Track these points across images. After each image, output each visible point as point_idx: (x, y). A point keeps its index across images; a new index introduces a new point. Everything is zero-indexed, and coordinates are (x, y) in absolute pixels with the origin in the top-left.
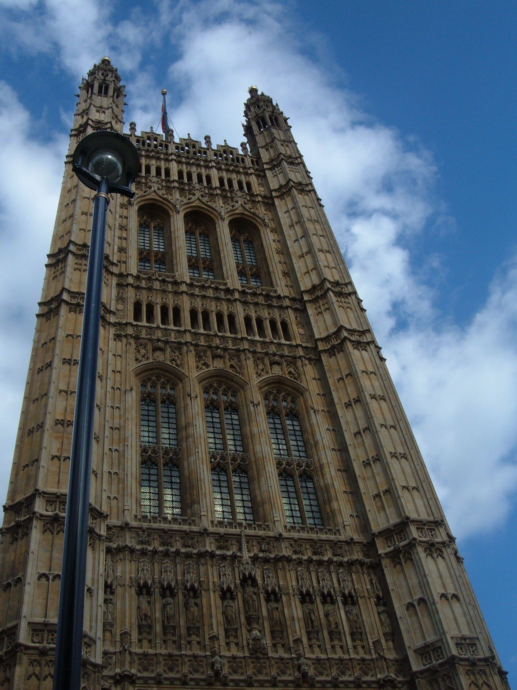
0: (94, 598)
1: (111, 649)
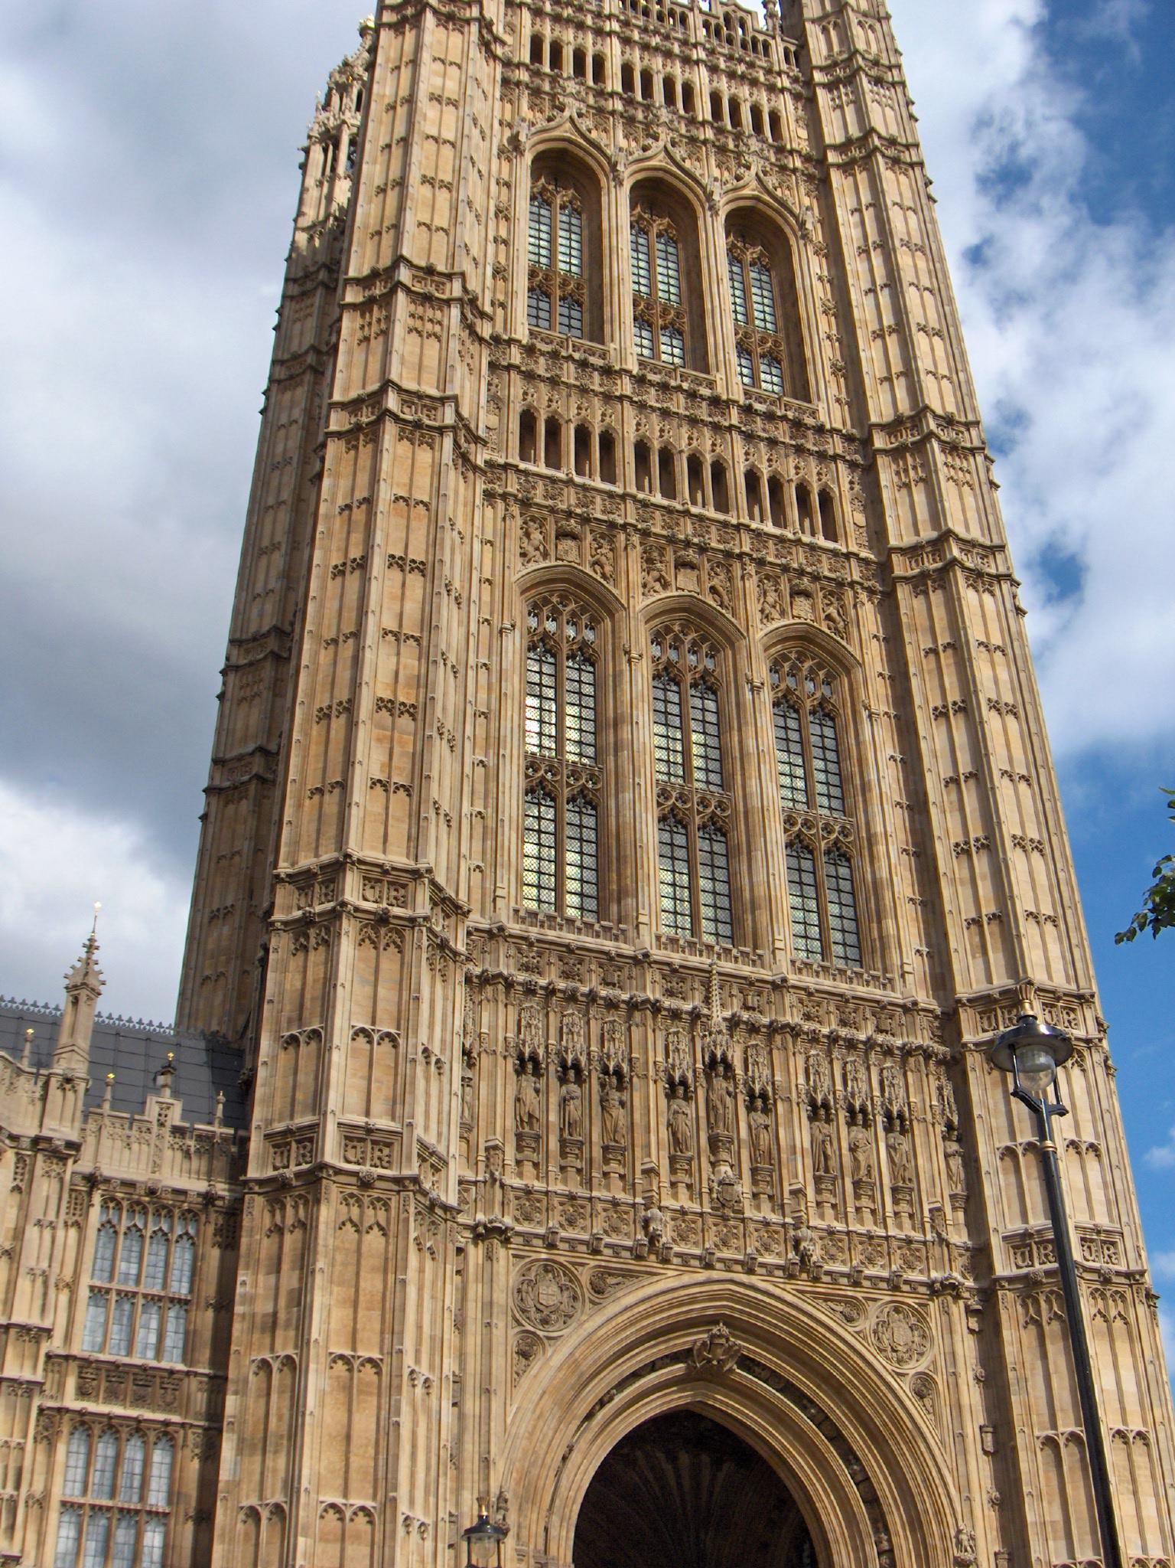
0: (445, 1079)
1: (470, 1176)
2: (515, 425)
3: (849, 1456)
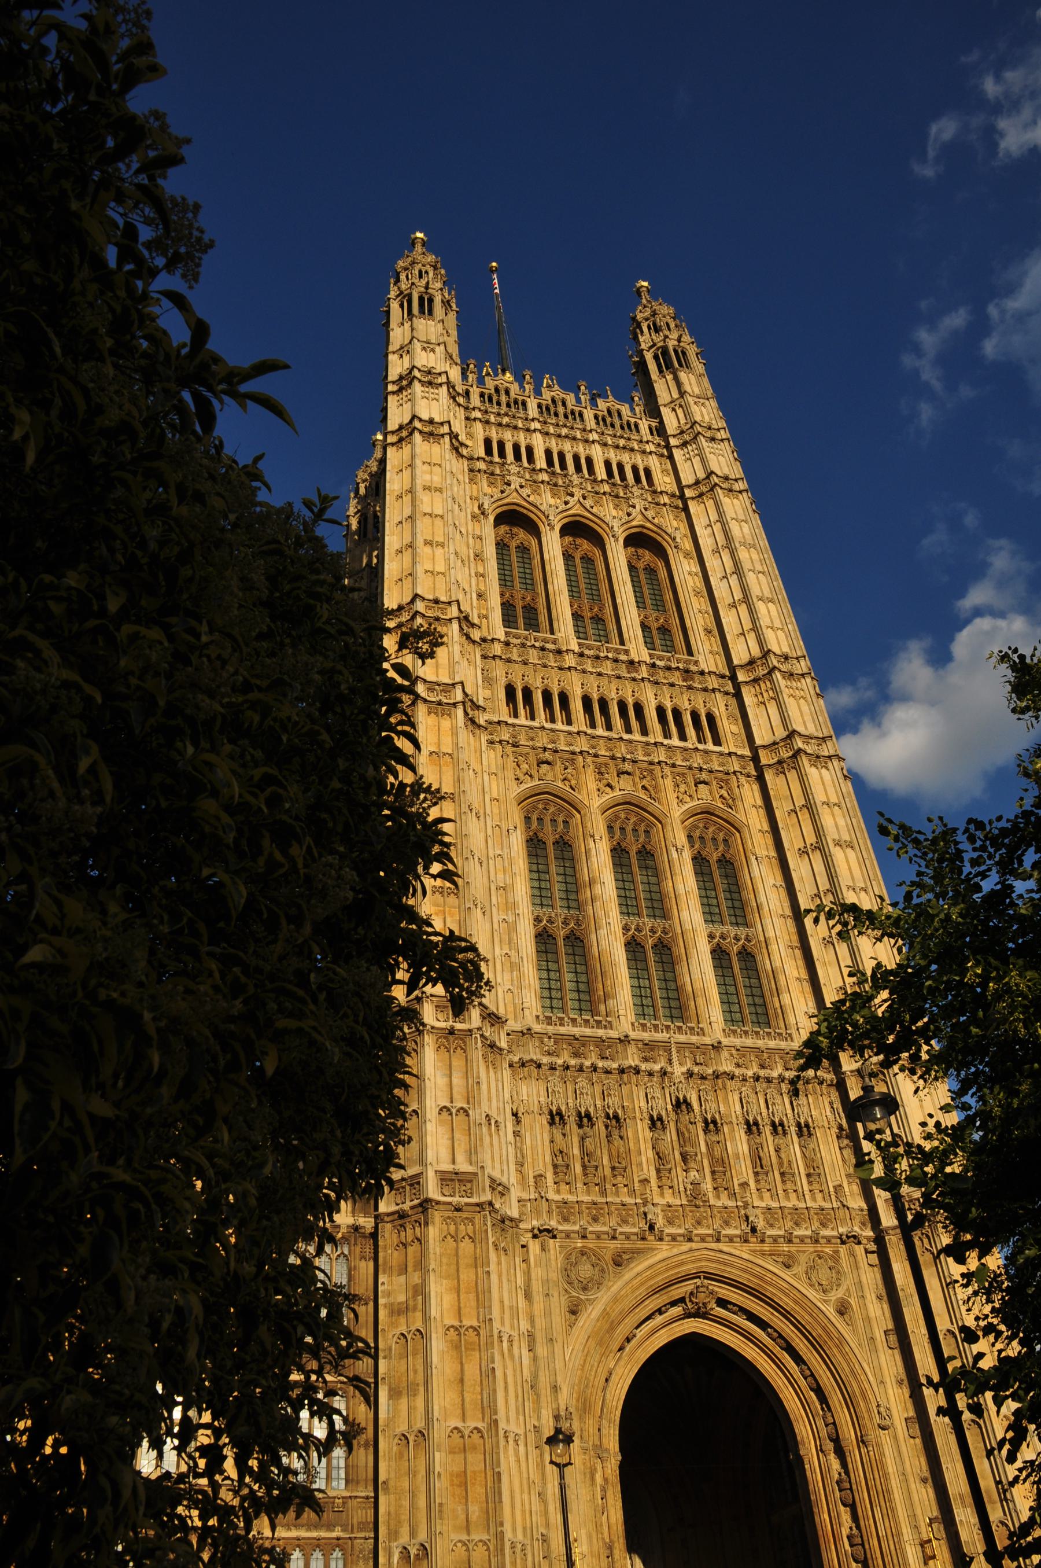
1: (525, 1196)
2: (502, 695)
3: (798, 1359)
